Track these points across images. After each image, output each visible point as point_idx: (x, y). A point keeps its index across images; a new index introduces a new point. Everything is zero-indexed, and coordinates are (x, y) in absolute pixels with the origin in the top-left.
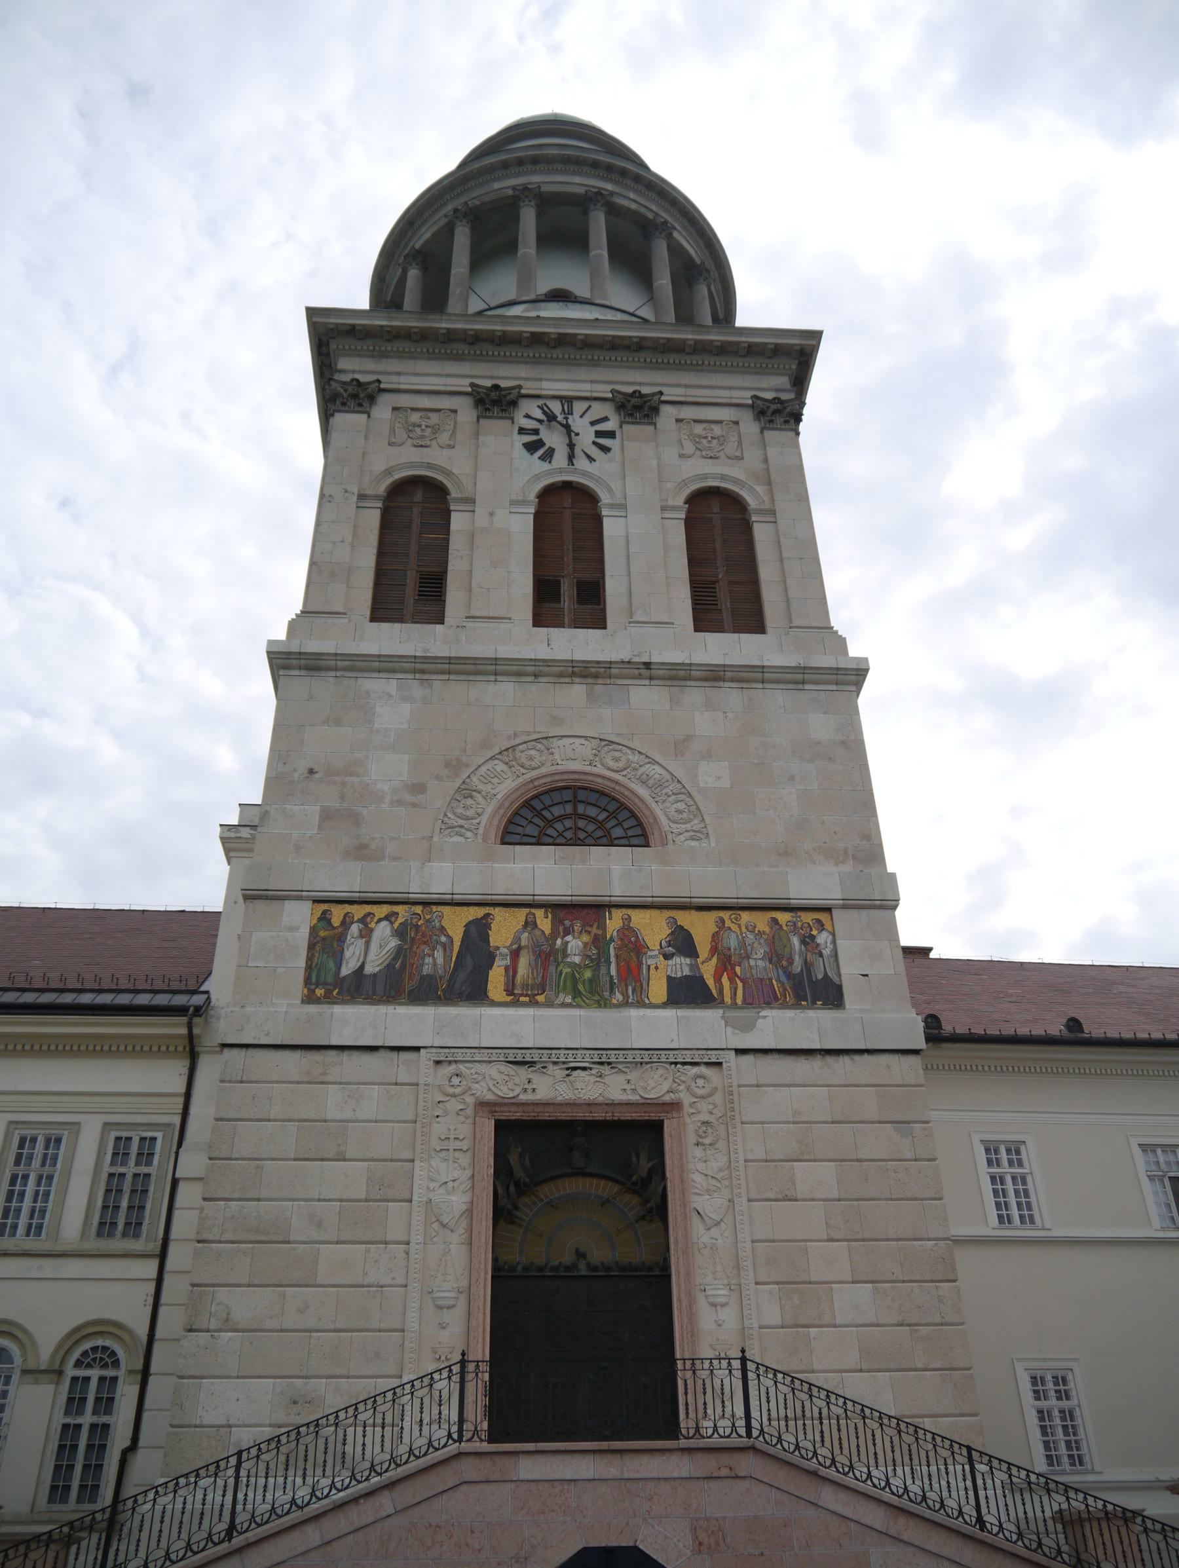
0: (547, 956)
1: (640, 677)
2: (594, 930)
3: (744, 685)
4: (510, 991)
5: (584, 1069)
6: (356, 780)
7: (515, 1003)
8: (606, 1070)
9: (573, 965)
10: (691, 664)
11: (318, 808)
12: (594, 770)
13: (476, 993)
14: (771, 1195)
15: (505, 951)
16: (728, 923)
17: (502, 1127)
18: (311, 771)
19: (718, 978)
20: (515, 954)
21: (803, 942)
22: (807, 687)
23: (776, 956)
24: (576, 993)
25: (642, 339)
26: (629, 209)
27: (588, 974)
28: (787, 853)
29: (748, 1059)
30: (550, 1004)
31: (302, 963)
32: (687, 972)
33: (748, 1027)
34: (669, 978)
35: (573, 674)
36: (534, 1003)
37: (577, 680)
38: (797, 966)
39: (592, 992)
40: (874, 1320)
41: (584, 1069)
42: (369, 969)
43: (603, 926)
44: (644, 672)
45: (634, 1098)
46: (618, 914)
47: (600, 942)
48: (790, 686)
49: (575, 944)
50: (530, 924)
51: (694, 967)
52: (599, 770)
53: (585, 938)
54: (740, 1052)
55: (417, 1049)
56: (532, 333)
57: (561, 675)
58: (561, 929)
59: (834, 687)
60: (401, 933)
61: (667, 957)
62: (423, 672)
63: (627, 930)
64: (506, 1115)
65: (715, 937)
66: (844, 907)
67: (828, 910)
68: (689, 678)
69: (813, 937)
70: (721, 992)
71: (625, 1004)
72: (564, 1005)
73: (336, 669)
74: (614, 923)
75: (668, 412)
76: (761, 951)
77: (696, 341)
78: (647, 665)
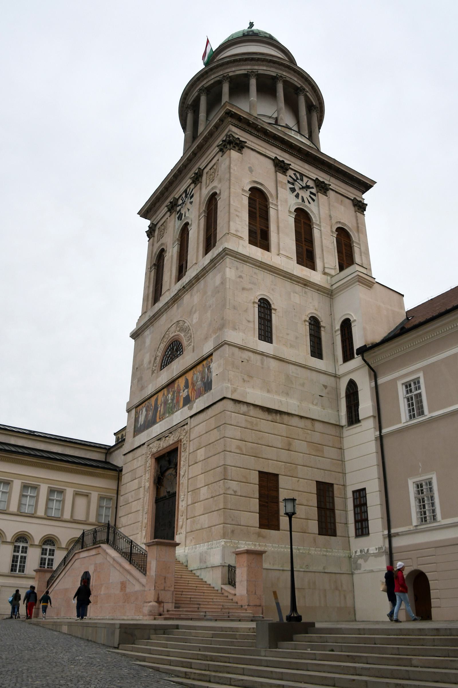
0: (166, 402)
1: (185, 292)
2: (173, 390)
3: (204, 277)
4: (160, 418)
5: (167, 436)
6: (142, 366)
7: (160, 421)
8: (170, 435)
10: (191, 280)
11: (137, 380)
12: (176, 334)
13: (153, 422)
14: (193, 463)
15: (160, 405)
16: (195, 372)
18: (137, 368)
19: (191, 394)
20: (161, 405)
21: (208, 369)
22: (217, 265)
23: (203, 378)
24: (169, 412)
25: (193, 152)
26: (212, 84)
27: (171, 405)
28: (206, 338)
29: (193, 419)
30: (165, 418)
31: (133, 427)
32: (187, 394)
33: (190, 409)
34: (184, 398)
35: (174, 302)
36: (163, 419)
37: (175, 303)
39: (172, 410)
40: (207, 498)
41: (167, 436)
42: (142, 423)
43: (174, 388)
44: (185, 290)
45: (174, 442)
46: (177, 381)
47: (173, 394)
48: (213, 268)
49: (170, 396)
50: (164, 394)
51: (188, 391)
52: (177, 333)
53: (172, 393)
54: (191, 417)
55: (144, 444)
56: (173, 176)
57: (172, 304)
58: (168, 393)
59: (222, 261)
60: (146, 410)
61: (184, 391)
62: (152, 322)
63: (178, 385)
64: (157, 456)
65: (193, 378)
66: (215, 351)
67: (211, 355)
68: (193, 284)
69: (210, 366)
70: (192, 397)
71: (176, 411)
73: (141, 333)
74: (176, 386)
75: (206, 171)
77: (203, 139)
78: (184, 287)
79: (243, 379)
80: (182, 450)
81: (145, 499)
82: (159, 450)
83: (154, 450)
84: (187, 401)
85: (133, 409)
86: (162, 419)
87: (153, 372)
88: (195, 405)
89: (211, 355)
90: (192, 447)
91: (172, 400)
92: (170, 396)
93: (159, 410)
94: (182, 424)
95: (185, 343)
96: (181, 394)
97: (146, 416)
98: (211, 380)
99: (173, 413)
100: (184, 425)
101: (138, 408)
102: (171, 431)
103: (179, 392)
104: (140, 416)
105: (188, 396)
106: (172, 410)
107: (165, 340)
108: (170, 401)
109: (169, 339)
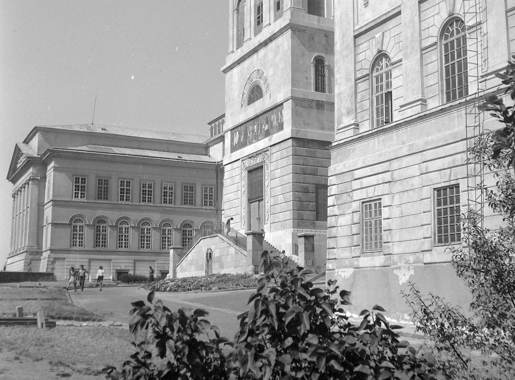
4: (249, 142)
9: (255, 132)
17: (250, 172)
23: (277, 119)
24: (256, 139)
33: (270, 140)
36: (251, 144)
38: (279, 121)
47: (258, 126)
54: (271, 146)
55: (239, 160)
60: (239, 134)
61: (265, 126)
66: (285, 102)
67: (282, 104)
72: (255, 142)
76: (276, 118)
79: (304, 122)
80: (266, 168)
81: (242, 198)
82: (250, 165)
83: (247, 165)
84: (268, 134)
85: (229, 131)
86: (251, 143)
87: (242, 106)
88: (273, 138)
89: (282, 104)
90: (272, 167)
91: (257, 130)
92: (255, 126)
93: (248, 135)
94: (265, 150)
95: (264, 89)
96: (263, 127)
97: (239, 138)
98: (283, 123)
99: (258, 141)
100: (266, 151)
101: (233, 131)
102: (258, 153)
103: (262, 125)
104: (235, 137)
105: (268, 130)
106: (257, 138)
107: (250, 82)
108: (256, 131)
109: (252, 82)
